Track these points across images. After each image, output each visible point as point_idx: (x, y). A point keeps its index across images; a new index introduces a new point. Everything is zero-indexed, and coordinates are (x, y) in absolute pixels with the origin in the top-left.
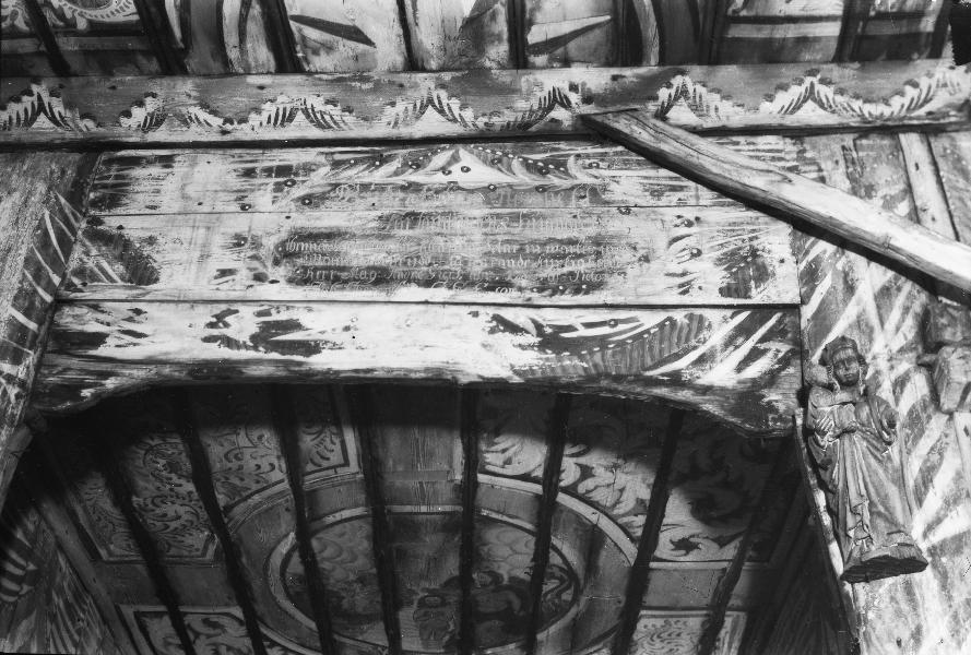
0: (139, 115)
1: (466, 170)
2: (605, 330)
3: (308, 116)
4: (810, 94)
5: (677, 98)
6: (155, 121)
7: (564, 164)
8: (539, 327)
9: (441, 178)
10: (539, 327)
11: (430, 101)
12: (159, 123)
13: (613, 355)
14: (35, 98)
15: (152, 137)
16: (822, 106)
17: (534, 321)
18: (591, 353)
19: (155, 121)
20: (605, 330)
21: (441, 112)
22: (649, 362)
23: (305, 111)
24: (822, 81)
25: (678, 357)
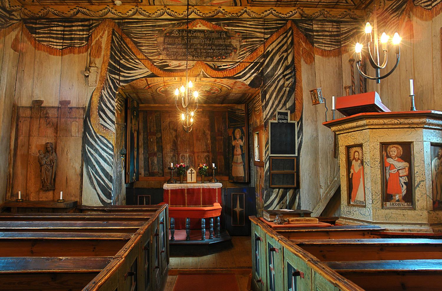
0: (131, 13)
1: (200, 26)
2: (227, 67)
3: (167, 13)
4: (271, 13)
5: (245, 12)
6: (134, 14)
7: (220, 25)
8: (215, 66)
9: (194, 28)
10: (215, 66)
11: (193, 11)
12: (135, 14)
13: (229, 72)
14: (108, 9)
15: (133, 17)
16: (273, 15)
17: (213, 64)
18: (224, 72)
19: (134, 14)
20: (227, 67)
21: (196, 13)
22: (235, 74)
23: (167, 13)
24: (273, 10)
25: (240, 73)
